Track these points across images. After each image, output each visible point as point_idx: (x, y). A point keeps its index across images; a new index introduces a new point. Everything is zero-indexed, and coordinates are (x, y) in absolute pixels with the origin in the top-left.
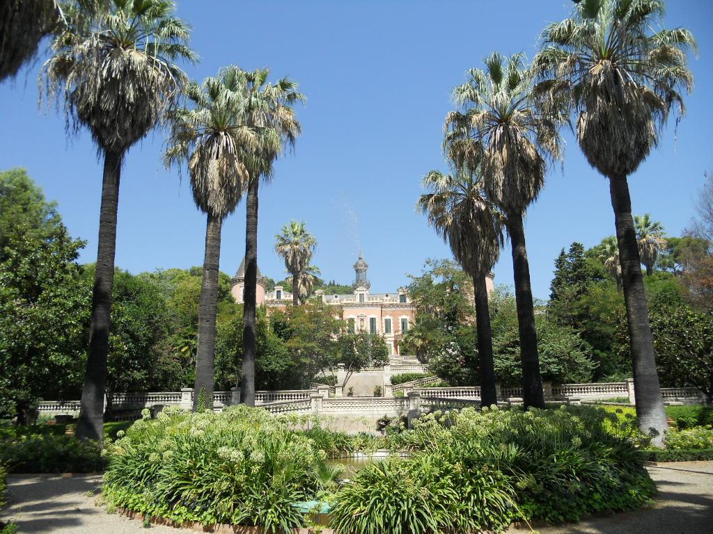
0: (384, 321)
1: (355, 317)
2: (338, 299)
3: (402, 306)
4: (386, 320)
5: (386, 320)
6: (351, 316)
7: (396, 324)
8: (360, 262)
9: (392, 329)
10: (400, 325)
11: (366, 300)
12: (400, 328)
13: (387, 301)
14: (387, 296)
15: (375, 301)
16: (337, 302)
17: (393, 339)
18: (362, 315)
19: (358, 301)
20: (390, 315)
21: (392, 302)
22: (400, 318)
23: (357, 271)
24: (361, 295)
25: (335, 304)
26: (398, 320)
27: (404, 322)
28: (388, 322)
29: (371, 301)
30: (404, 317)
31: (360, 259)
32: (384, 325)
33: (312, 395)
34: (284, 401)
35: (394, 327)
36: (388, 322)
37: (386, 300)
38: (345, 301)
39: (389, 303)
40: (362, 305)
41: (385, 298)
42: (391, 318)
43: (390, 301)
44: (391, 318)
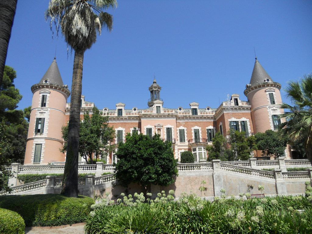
0: (178, 132)
1: (152, 127)
2: (136, 111)
3: (194, 118)
4: (180, 131)
5: (180, 131)
6: (149, 126)
7: (189, 134)
8: (155, 85)
9: (186, 138)
10: (193, 135)
12: (193, 138)
13: (180, 113)
14: (180, 109)
16: (136, 114)
17: (187, 147)
18: (159, 125)
19: (155, 112)
20: (184, 126)
21: (184, 115)
22: (193, 128)
23: (152, 92)
25: (134, 115)
26: (191, 130)
27: (196, 133)
29: (167, 113)
30: (196, 127)
32: (178, 135)
35: (187, 137)
36: (182, 132)
37: (180, 113)
38: (143, 113)
39: (182, 115)
40: (159, 116)
42: (185, 129)
43: (183, 114)
44: (185, 129)
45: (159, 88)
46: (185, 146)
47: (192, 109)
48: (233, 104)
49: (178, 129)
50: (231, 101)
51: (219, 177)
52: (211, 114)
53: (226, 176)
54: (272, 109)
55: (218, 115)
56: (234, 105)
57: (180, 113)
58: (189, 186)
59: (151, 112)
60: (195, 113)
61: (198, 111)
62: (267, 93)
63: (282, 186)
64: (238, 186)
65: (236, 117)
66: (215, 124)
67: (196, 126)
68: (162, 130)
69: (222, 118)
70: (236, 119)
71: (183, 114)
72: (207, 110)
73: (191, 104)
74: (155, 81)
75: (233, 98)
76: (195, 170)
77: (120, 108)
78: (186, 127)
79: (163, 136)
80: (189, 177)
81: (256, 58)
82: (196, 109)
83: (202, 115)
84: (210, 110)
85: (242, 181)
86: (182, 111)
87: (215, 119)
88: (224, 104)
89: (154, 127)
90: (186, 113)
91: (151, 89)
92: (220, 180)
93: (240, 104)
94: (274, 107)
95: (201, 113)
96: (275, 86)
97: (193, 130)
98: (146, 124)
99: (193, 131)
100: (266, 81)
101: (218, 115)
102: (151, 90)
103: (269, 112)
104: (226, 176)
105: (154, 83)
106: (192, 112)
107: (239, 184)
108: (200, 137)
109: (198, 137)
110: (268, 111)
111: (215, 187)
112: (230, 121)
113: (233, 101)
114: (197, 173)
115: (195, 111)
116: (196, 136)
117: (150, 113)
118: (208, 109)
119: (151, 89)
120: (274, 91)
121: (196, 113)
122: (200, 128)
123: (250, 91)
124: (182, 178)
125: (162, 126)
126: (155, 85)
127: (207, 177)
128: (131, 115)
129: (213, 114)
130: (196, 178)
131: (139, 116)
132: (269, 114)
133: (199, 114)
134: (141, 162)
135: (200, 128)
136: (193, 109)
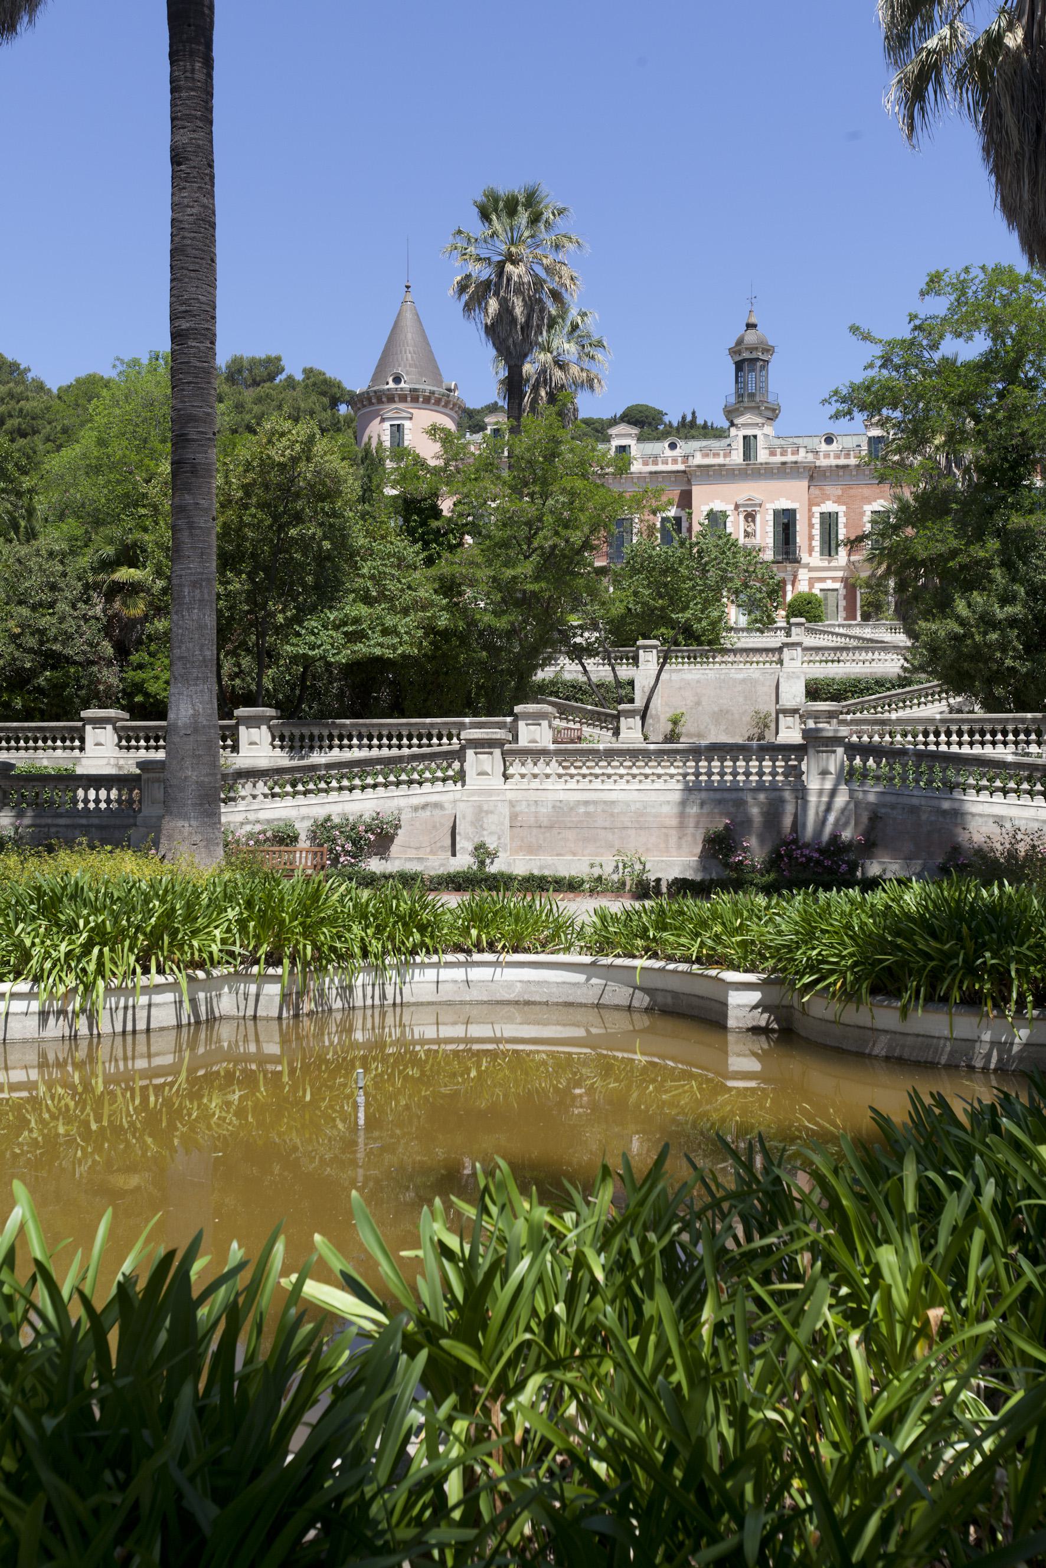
0: (816, 521)
1: (729, 508)
2: (677, 452)
6: (718, 506)
11: (762, 456)
14: (829, 440)
15: (789, 458)
16: (675, 461)
19: (737, 457)
20: (838, 501)
21: (842, 461)
23: (739, 366)
24: (749, 442)
28: (829, 522)
29: (778, 459)
31: (750, 326)
32: (816, 532)
33: (466, 734)
34: (406, 751)
36: (829, 522)
37: (827, 456)
38: (698, 460)
39: (833, 462)
41: (824, 447)
42: (841, 509)
44: (841, 509)
46: (835, 569)
49: (815, 509)
57: (827, 456)
59: (725, 456)
68: (758, 517)
71: (838, 457)
78: (844, 504)
79: (763, 538)
86: (834, 446)
89: (732, 507)
98: (706, 500)
105: (750, 326)
117: (720, 460)
125: (760, 505)
126: (751, 337)
128: (661, 467)
131: (684, 472)
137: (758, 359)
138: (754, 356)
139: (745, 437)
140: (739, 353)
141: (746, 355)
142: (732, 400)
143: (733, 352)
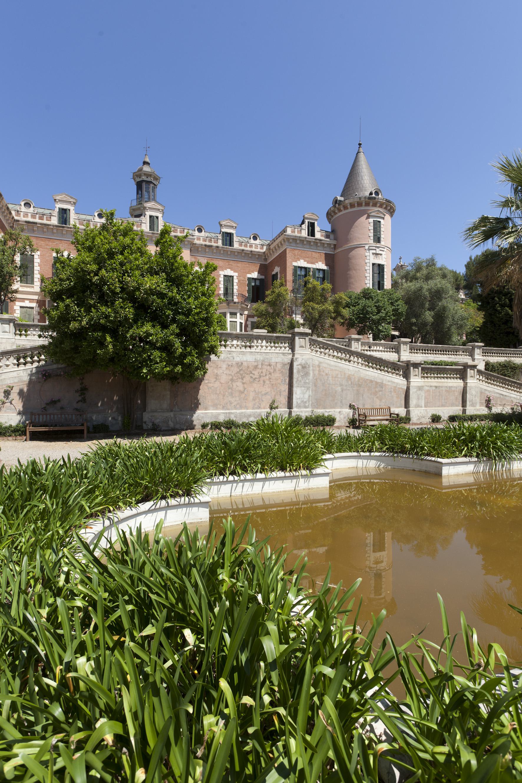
8: (146, 169)
14: (200, 230)
21: (208, 243)
22: (222, 273)
23: (139, 185)
30: (229, 272)
31: (145, 163)
39: (201, 242)
43: (205, 241)
45: (156, 179)
47: (223, 232)
48: (304, 233)
50: (303, 226)
51: (304, 367)
52: (258, 250)
53: (319, 366)
54: (374, 251)
55: (273, 252)
56: (306, 236)
57: (199, 239)
58: (239, 384)
60: (228, 243)
61: (235, 239)
62: (371, 220)
63: (419, 392)
64: (339, 389)
65: (307, 259)
66: (264, 269)
67: (229, 270)
69: (282, 260)
70: (308, 263)
72: (252, 241)
73: (223, 223)
74: (147, 160)
75: (307, 221)
76: (253, 350)
77: (65, 206)
80: (240, 365)
81: (360, 144)
82: (230, 235)
83: (243, 248)
84: (258, 242)
85: (349, 378)
86: (203, 234)
87: (266, 260)
88: (289, 231)
90: (210, 241)
91: (137, 176)
92: (307, 374)
93: (318, 235)
94: (377, 250)
95: (241, 245)
96: (386, 208)
97: (222, 276)
99: (222, 279)
100: (374, 195)
101: (273, 252)
102: (138, 180)
103: (368, 257)
104: (319, 366)
105: (145, 163)
106: (223, 240)
107: (341, 385)
108: (235, 291)
109: (229, 291)
110: (367, 254)
111: (295, 389)
112: (295, 267)
113: (305, 226)
114: (259, 357)
115: (228, 238)
116: (226, 289)
118: (255, 238)
119: (137, 176)
120: (383, 218)
121: (231, 244)
122: (235, 274)
123: (340, 210)
124: (224, 366)
126: (146, 169)
127: (279, 366)
129: (262, 248)
130: (256, 367)
132: (367, 261)
133: (236, 245)
134: (129, 312)
135: (235, 274)
136: (226, 233)
137: (151, 182)
138: (149, 179)
139: (151, 217)
140: (140, 176)
141: (144, 178)
142: (135, 203)
143: (137, 174)
